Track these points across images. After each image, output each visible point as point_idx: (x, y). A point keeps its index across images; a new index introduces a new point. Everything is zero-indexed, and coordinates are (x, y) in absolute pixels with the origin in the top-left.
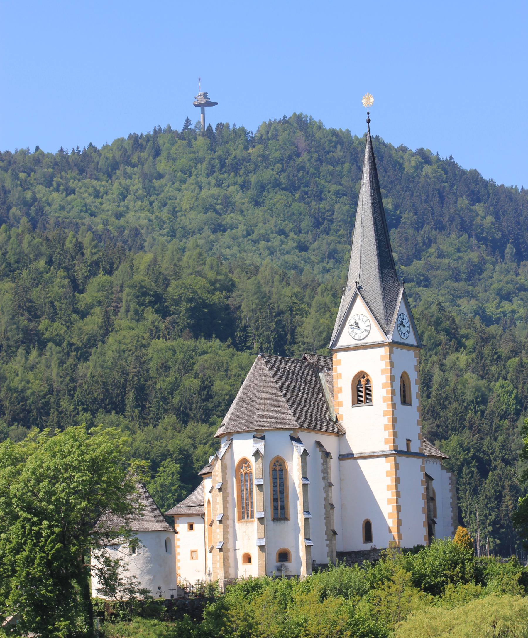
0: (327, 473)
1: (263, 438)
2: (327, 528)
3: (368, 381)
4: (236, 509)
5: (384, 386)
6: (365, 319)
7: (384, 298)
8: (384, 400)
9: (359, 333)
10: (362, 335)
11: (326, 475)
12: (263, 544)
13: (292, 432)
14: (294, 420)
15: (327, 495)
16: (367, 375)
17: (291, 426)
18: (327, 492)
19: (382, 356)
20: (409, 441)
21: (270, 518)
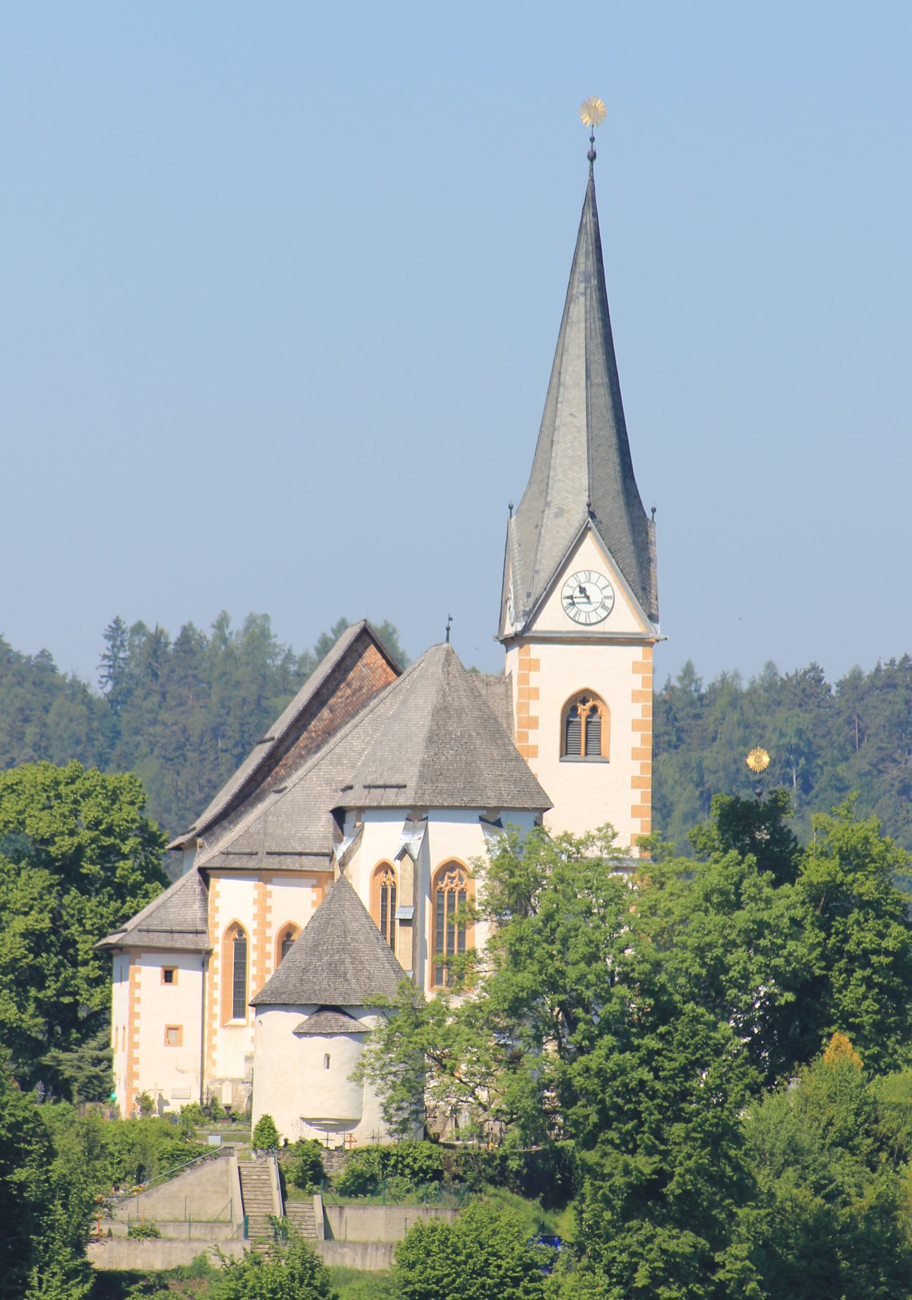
1: (498, 824)
3: (594, 709)
4: (427, 964)
5: (636, 725)
6: (602, 583)
7: (635, 543)
8: (636, 754)
9: (588, 613)
10: (593, 615)
16: (596, 696)
19: (635, 664)
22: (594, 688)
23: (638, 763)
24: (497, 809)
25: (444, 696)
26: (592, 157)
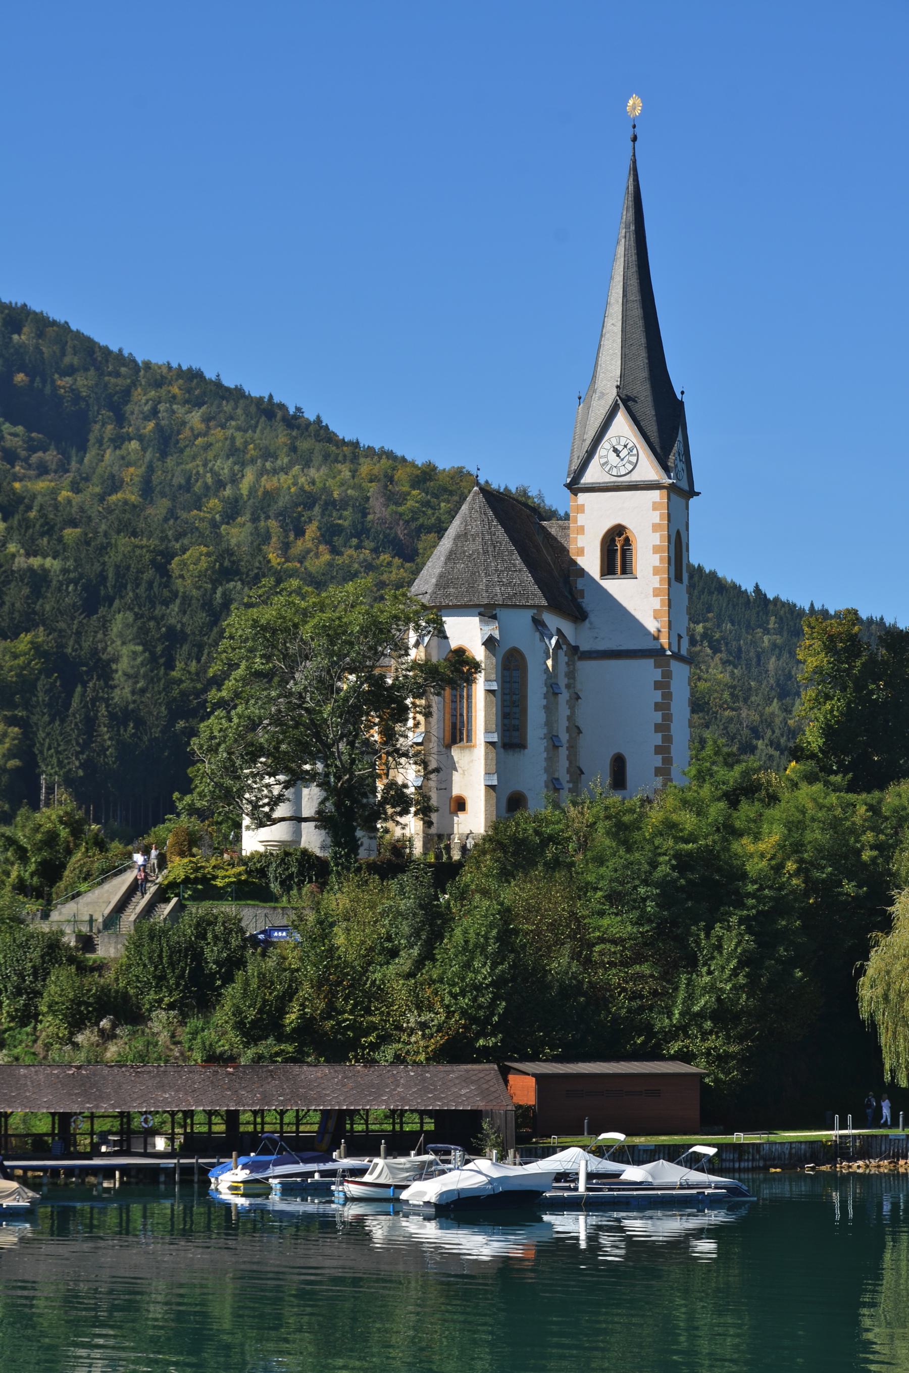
0: (574, 678)
1: (494, 617)
2: (570, 763)
3: (627, 541)
8: (656, 571)
10: (622, 469)
11: (572, 681)
12: (495, 783)
13: (535, 611)
14: (539, 592)
15: (573, 713)
17: (537, 602)
18: (572, 708)
20: (680, 637)
21: (500, 744)
22: (624, 523)
23: (657, 578)
24: (495, 606)
25: (466, 525)
26: (634, 139)
